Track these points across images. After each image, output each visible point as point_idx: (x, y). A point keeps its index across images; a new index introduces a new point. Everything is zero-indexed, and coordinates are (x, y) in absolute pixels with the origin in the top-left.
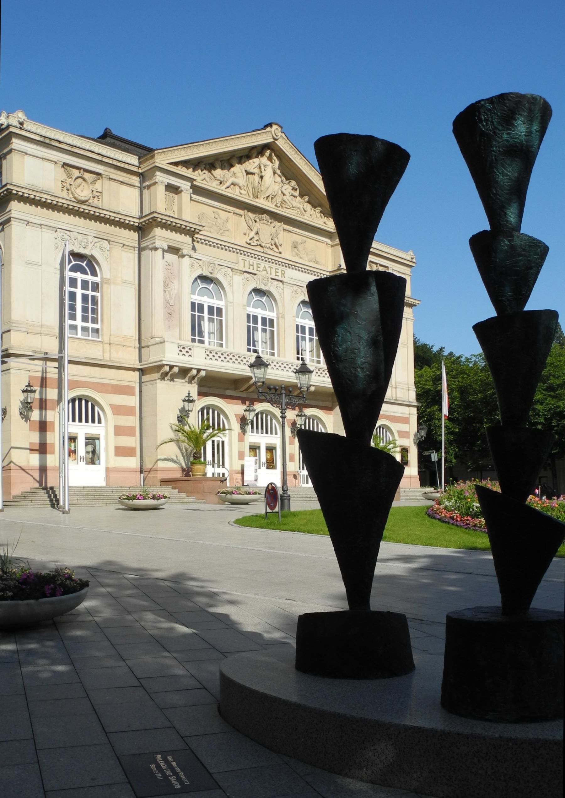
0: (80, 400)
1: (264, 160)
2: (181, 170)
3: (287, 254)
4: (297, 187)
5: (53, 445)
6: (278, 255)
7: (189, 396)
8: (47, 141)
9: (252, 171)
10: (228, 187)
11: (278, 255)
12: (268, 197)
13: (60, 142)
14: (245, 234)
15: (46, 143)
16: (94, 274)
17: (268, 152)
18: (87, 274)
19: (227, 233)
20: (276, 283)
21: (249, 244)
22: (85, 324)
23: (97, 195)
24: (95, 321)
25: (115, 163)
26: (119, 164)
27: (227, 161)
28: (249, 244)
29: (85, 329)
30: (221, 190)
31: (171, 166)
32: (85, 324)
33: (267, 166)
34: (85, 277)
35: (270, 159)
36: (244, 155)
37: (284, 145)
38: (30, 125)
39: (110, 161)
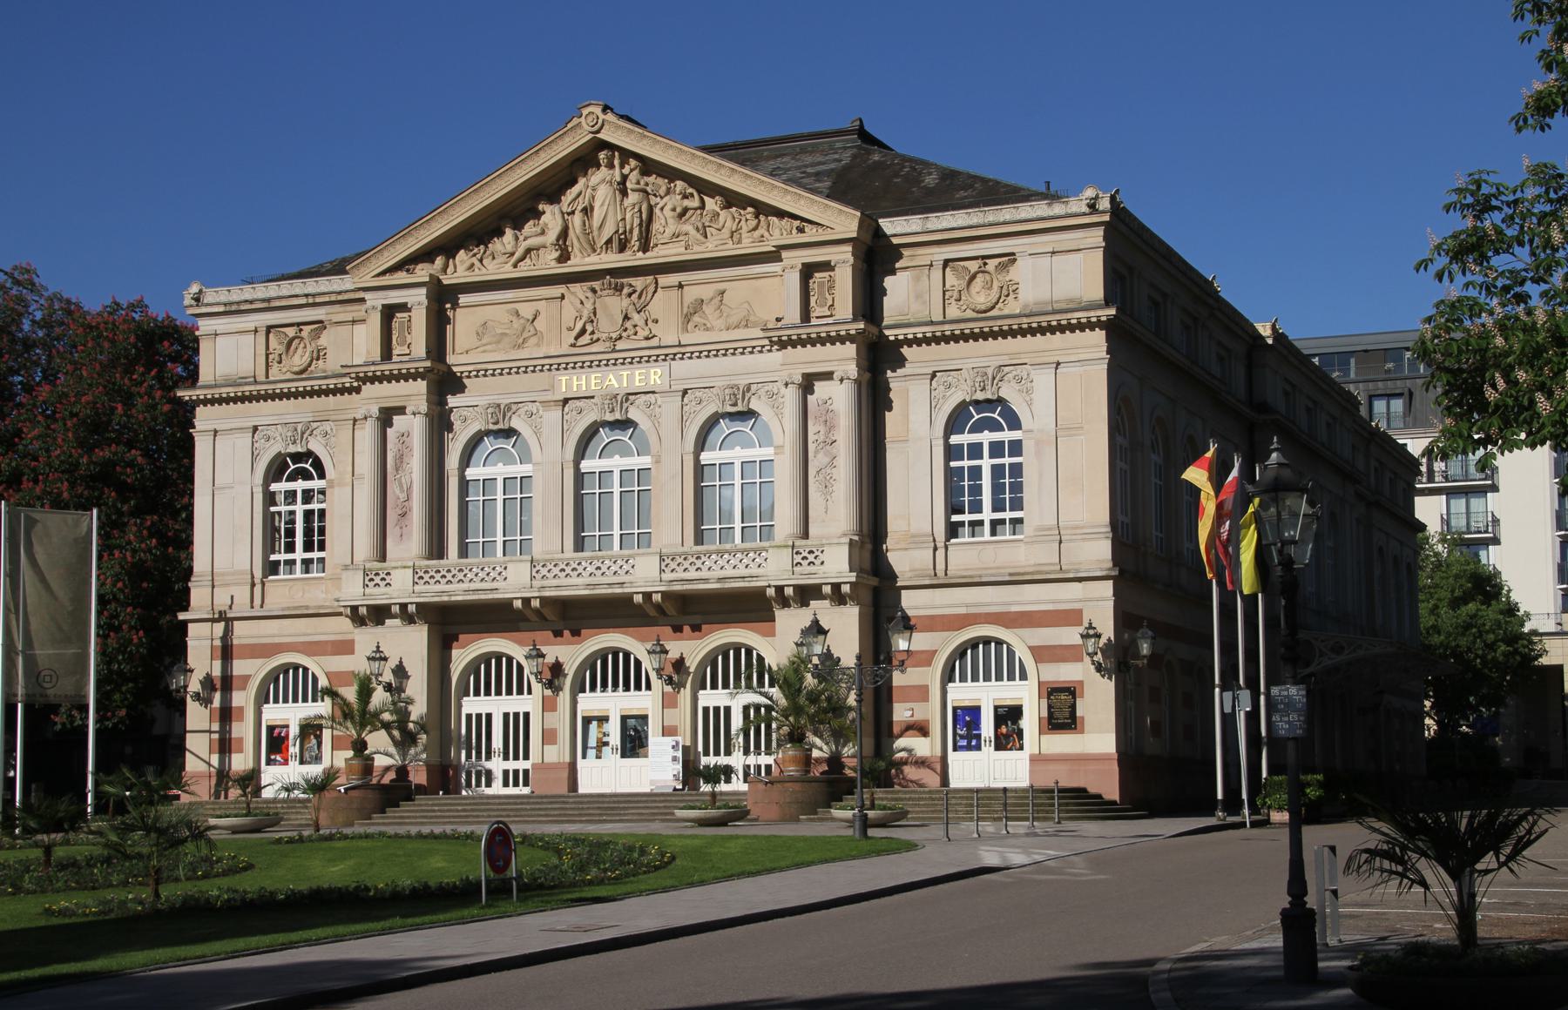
0: (286, 672)
1: (599, 176)
2: (401, 277)
3: (668, 334)
4: (690, 190)
5: (241, 740)
6: (645, 344)
7: (378, 650)
8: (234, 308)
9: (565, 209)
10: (522, 259)
11: (645, 344)
12: (609, 241)
13: (251, 302)
14: (570, 329)
15: (232, 310)
16: (322, 476)
17: (602, 155)
18: (312, 478)
19: (533, 340)
20: (643, 398)
21: (573, 345)
22: (309, 555)
23: (319, 355)
24: (322, 547)
25: (333, 298)
26: (340, 298)
27: (517, 211)
28: (573, 345)
29: (307, 563)
30: (507, 272)
31: (387, 276)
32: (309, 555)
33: (597, 185)
34: (308, 484)
35: (611, 166)
36: (553, 185)
37: (618, 134)
38: (210, 296)
39: (326, 299)
